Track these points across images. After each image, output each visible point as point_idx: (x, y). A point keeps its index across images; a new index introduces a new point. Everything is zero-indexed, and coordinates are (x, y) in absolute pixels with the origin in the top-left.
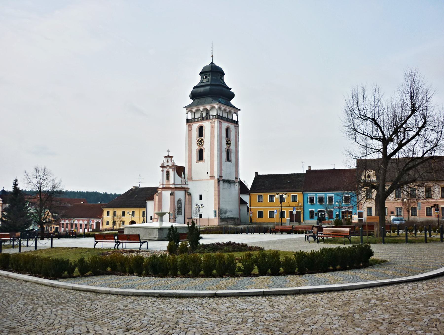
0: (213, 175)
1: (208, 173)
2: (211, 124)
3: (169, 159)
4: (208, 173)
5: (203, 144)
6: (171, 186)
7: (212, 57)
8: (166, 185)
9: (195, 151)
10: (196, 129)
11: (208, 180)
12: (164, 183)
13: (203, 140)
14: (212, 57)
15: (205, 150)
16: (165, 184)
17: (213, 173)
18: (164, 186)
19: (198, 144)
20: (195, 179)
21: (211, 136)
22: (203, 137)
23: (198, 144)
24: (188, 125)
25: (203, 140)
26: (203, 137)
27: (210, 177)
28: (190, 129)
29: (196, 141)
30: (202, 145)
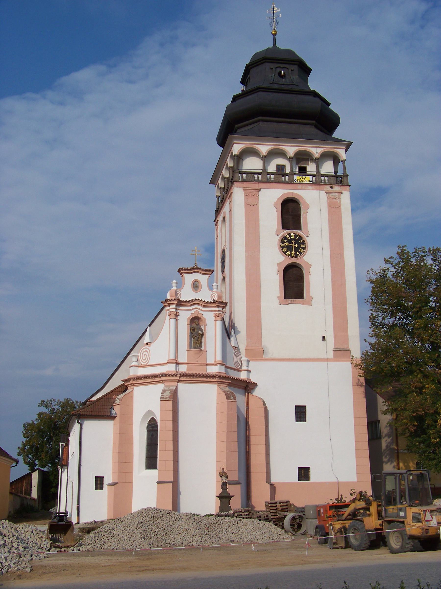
0: (345, 346)
1: (324, 337)
2: (329, 198)
3: (203, 279)
4: (324, 337)
5: (301, 250)
6: (214, 370)
7: (274, 35)
8: (191, 366)
9: (276, 268)
10: (275, 205)
11: (327, 360)
12: (183, 358)
14: (274, 35)
15: (311, 270)
16: (186, 361)
17: (346, 339)
18: (183, 369)
19: (285, 249)
20: (276, 356)
21: (330, 231)
22: (300, 229)
23: (285, 249)
24: (245, 189)
25: (300, 238)
26: (300, 229)
27: (336, 350)
28: (251, 200)
29: (277, 239)
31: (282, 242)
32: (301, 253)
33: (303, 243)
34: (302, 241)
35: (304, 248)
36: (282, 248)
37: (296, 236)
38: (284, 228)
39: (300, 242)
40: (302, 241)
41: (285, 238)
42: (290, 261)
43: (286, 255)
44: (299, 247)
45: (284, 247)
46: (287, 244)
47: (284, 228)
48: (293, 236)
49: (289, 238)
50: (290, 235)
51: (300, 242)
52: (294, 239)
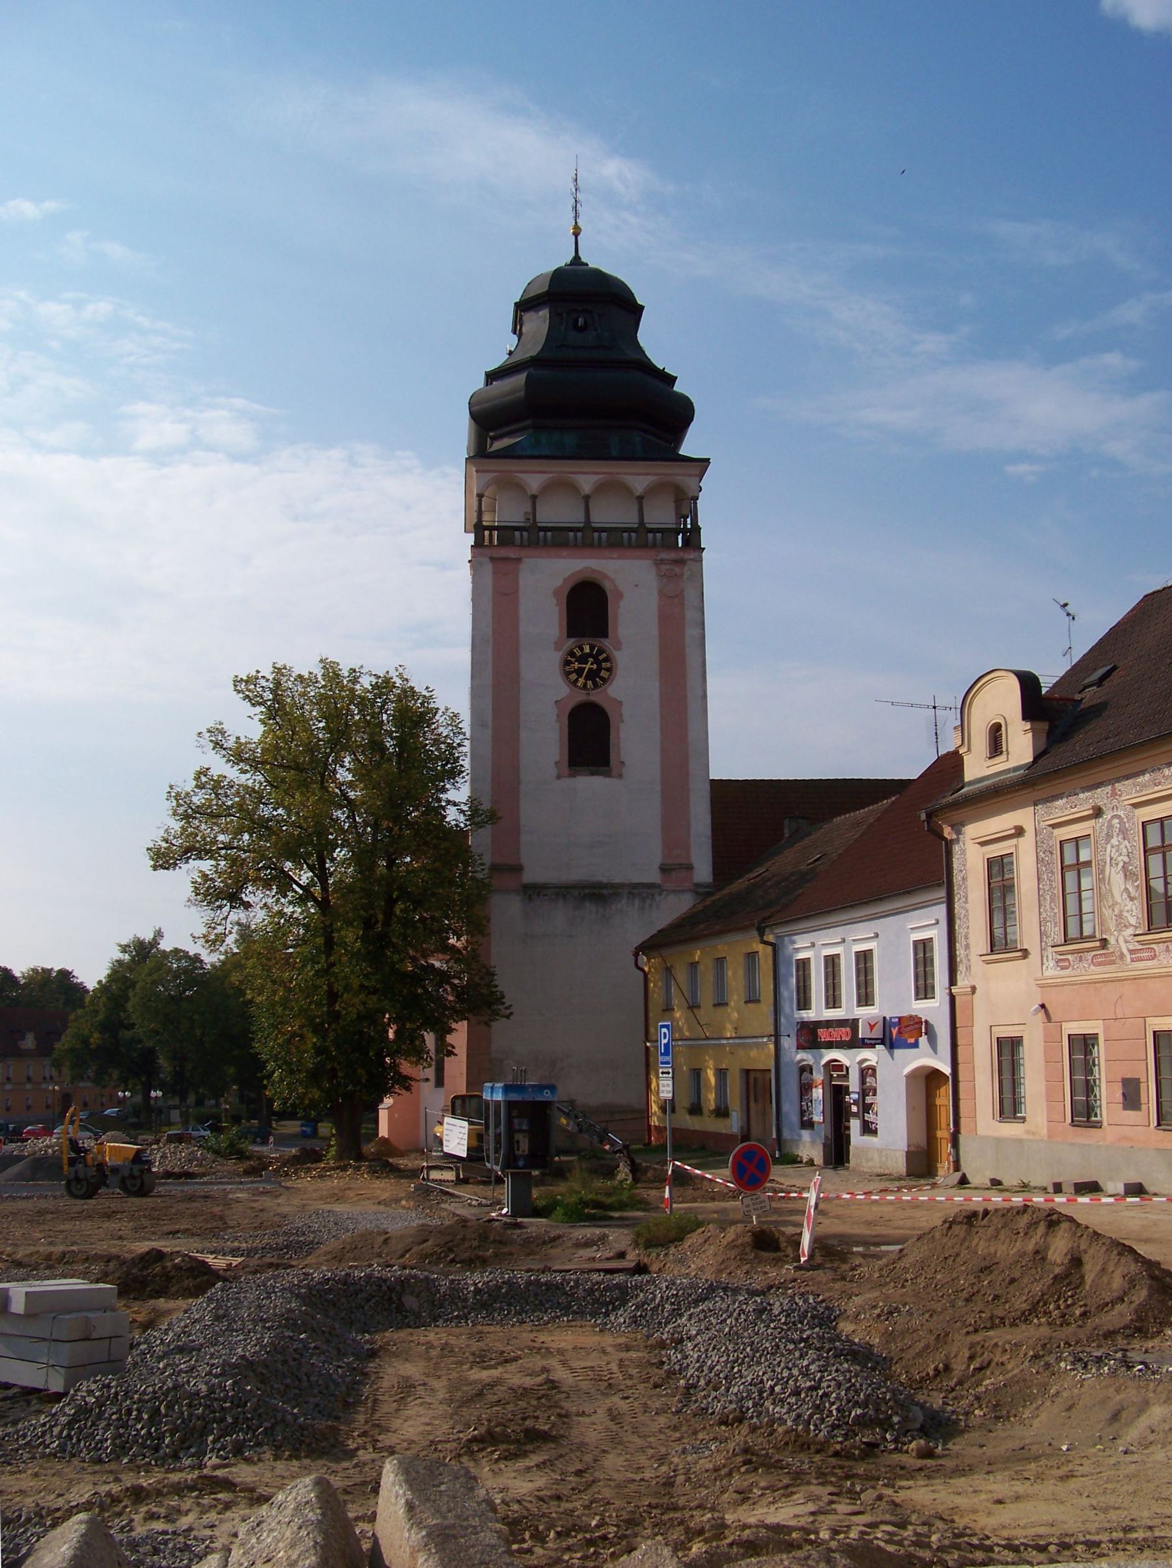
5: (604, 674)
13: (601, 652)
19: (574, 676)
23: (574, 676)
30: (603, 679)
31: (567, 663)
32: (604, 680)
33: (607, 659)
34: (605, 655)
35: (609, 670)
36: (567, 674)
37: (592, 647)
38: (570, 635)
39: (601, 658)
40: (605, 655)
41: (572, 654)
42: (581, 697)
43: (576, 686)
44: (600, 669)
45: (570, 673)
46: (576, 665)
47: (570, 635)
48: (587, 649)
49: (578, 654)
50: (581, 649)
51: (601, 658)
52: (590, 655)
